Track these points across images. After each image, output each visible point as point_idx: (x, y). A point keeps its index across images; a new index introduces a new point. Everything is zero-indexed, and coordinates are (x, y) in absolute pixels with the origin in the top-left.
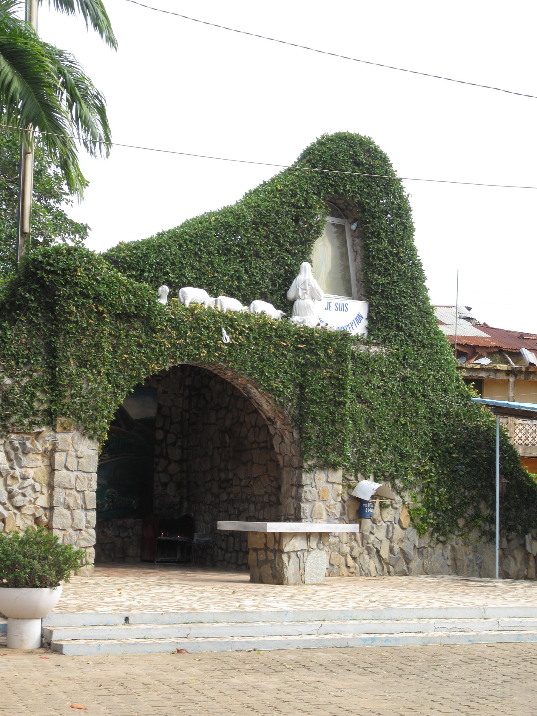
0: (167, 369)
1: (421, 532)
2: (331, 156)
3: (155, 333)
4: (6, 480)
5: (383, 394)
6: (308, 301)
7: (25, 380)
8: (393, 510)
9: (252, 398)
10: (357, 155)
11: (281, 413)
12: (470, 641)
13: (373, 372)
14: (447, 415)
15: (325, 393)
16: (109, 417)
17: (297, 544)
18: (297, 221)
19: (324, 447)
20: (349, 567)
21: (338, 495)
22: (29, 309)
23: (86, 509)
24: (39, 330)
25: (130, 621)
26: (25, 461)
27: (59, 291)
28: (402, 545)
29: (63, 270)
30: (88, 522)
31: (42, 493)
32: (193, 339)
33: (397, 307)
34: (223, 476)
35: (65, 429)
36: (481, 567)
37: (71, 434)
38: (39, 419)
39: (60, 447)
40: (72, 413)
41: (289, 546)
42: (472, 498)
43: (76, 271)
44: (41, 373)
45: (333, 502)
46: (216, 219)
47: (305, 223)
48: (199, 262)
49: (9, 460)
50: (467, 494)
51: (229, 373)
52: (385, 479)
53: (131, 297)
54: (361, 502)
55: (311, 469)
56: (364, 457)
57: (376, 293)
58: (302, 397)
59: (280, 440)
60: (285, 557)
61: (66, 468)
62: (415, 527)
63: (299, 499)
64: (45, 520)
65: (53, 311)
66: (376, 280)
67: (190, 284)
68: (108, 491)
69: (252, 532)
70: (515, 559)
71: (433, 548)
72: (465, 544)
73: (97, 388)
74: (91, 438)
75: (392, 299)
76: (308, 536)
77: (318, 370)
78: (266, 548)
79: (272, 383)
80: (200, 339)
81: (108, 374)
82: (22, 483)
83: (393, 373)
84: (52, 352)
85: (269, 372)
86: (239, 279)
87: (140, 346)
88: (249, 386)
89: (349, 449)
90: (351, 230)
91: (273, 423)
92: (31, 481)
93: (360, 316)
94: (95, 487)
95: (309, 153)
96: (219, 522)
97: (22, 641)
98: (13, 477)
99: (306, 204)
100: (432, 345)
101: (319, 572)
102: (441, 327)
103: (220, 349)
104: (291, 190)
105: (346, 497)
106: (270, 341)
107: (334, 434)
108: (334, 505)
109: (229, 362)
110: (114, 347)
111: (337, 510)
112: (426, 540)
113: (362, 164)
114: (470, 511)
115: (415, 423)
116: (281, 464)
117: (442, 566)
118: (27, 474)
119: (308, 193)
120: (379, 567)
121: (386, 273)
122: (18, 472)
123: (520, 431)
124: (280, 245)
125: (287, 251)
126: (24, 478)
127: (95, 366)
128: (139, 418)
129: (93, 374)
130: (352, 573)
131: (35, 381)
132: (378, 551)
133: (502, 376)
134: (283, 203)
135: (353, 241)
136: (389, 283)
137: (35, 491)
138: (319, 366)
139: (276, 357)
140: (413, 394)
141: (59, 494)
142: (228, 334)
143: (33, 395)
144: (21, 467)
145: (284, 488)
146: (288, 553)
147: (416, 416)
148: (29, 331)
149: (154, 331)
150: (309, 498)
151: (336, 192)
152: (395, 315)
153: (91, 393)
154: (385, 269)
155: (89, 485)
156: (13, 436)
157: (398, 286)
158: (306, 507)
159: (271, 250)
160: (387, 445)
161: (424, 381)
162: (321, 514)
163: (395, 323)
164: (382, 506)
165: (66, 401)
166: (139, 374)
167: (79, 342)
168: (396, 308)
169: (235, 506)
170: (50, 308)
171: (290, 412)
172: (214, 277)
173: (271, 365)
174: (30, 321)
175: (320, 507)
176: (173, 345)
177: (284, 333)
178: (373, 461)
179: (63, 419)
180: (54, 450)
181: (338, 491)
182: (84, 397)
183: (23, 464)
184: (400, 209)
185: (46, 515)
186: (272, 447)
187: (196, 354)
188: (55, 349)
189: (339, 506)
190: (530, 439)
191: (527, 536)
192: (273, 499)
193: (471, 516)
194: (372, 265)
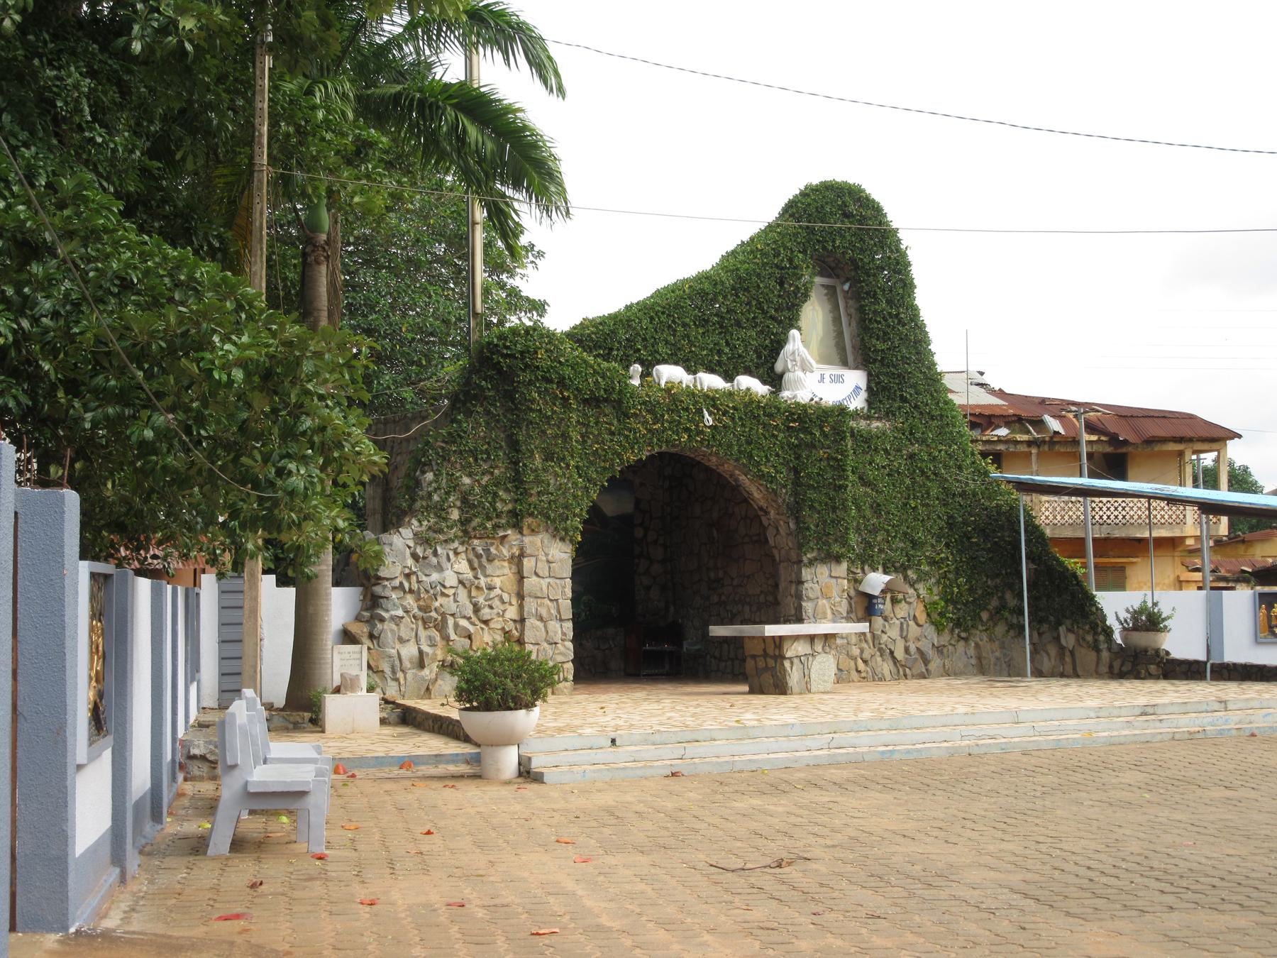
0: (644, 458)
1: (939, 629)
2: (817, 208)
3: (629, 418)
4: (470, 592)
5: (889, 475)
6: (800, 374)
7: (486, 478)
8: (907, 606)
9: (740, 486)
10: (846, 206)
11: (775, 501)
13: (876, 450)
14: (963, 494)
15: (822, 476)
16: (581, 515)
18: (781, 284)
19: (825, 538)
21: (844, 591)
22: (486, 398)
23: (561, 620)
24: (498, 421)
25: (618, 743)
26: (490, 569)
27: (519, 376)
28: (919, 644)
29: (522, 353)
30: (564, 634)
31: (511, 604)
32: (670, 423)
33: (899, 376)
34: (712, 575)
35: (533, 530)
37: (540, 536)
38: (503, 521)
39: (528, 552)
40: (540, 513)
41: (792, 650)
42: (996, 587)
43: (536, 353)
44: (502, 470)
45: (838, 599)
46: (690, 287)
47: (791, 285)
48: (674, 335)
49: (473, 569)
50: (989, 583)
51: (714, 459)
52: (896, 571)
53: (600, 380)
54: (869, 598)
55: (811, 563)
56: (871, 547)
57: (875, 360)
58: (797, 483)
59: (775, 531)
60: (787, 664)
61: (537, 574)
62: (933, 623)
63: (799, 597)
64: (516, 634)
65: (513, 400)
66: (874, 346)
67: (665, 362)
68: (584, 598)
69: (749, 637)
70: (1048, 654)
72: (991, 640)
73: (566, 484)
74: (562, 539)
75: (894, 366)
76: (812, 638)
77: (814, 451)
78: (765, 655)
79: (763, 468)
80: (679, 422)
81: (577, 467)
82: (489, 594)
83: (899, 450)
84: (514, 445)
85: (758, 456)
86: (720, 352)
87: (612, 433)
88: (737, 472)
89: (853, 538)
90: (843, 291)
91: (767, 513)
92: (498, 591)
93: (857, 388)
94: (570, 595)
95: (792, 207)
97: (498, 770)
98: (478, 588)
99: (791, 264)
100: (941, 416)
101: (826, 678)
102: (950, 396)
103: (702, 432)
104: (773, 249)
105: (852, 593)
106: (758, 421)
107: (836, 522)
108: (840, 602)
109: (713, 446)
110: (582, 436)
111: (843, 608)
112: (946, 637)
113: (853, 216)
114: (995, 603)
115: (927, 505)
116: (777, 558)
117: (965, 666)
118: (493, 584)
119: (792, 252)
120: (894, 670)
121: (885, 337)
122: (483, 581)
123: (1047, 509)
124: (764, 312)
125: (772, 318)
126: (491, 588)
127: (563, 459)
128: (615, 515)
129: (561, 468)
131: (496, 478)
132: (892, 653)
133: (1023, 448)
134: (764, 264)
135: (847, 303)
136: (889, 349)
137: (503, 602)
138: (814, 447)
139: (766, 438)
140: (923, 472)
141: (530, 604)
142: (710, 415)
143: (495, 495)
144: (486, 576)
145: (782, 586)
147: (928, 498)
148: (487, 424)
149: (627, 416)
150: (811, 595)
151: (824, 248)
152: (898, 384)
153: (560, 489)
154: (884, 332)
155: (563, 593)
156: (476, 542)
157: (899, 351)
158: (808, 606)
159: (754, 318)
160: (896, 531)
161: (935, 458)
162: (825, 613)
163: (898, 393)
164: (894, 601)
165: (533, 499)
166: (613, 465)
167: (544, 432)
168: (899, 376)
169: (728, 608)
170: (509, 396)
171: (784, 500)
172: (691, 351)
173: (761, 448)
174: (488, 412)
175: (824, 605)
176: (650, 431)
177: (774, 411)
178: (881, 551)
179: (530, 520)
180: (522, 555)
182: (552, 494)
183: (488, 573)
184: (898, 263)
185: (516, 629)
186: (767, 541)
187: (675, 440)
188: (517, 442)
189: (845, 603)
190: (1059, 517)
192: (770, 598)
193: (996, 608)
194: (869, 329)
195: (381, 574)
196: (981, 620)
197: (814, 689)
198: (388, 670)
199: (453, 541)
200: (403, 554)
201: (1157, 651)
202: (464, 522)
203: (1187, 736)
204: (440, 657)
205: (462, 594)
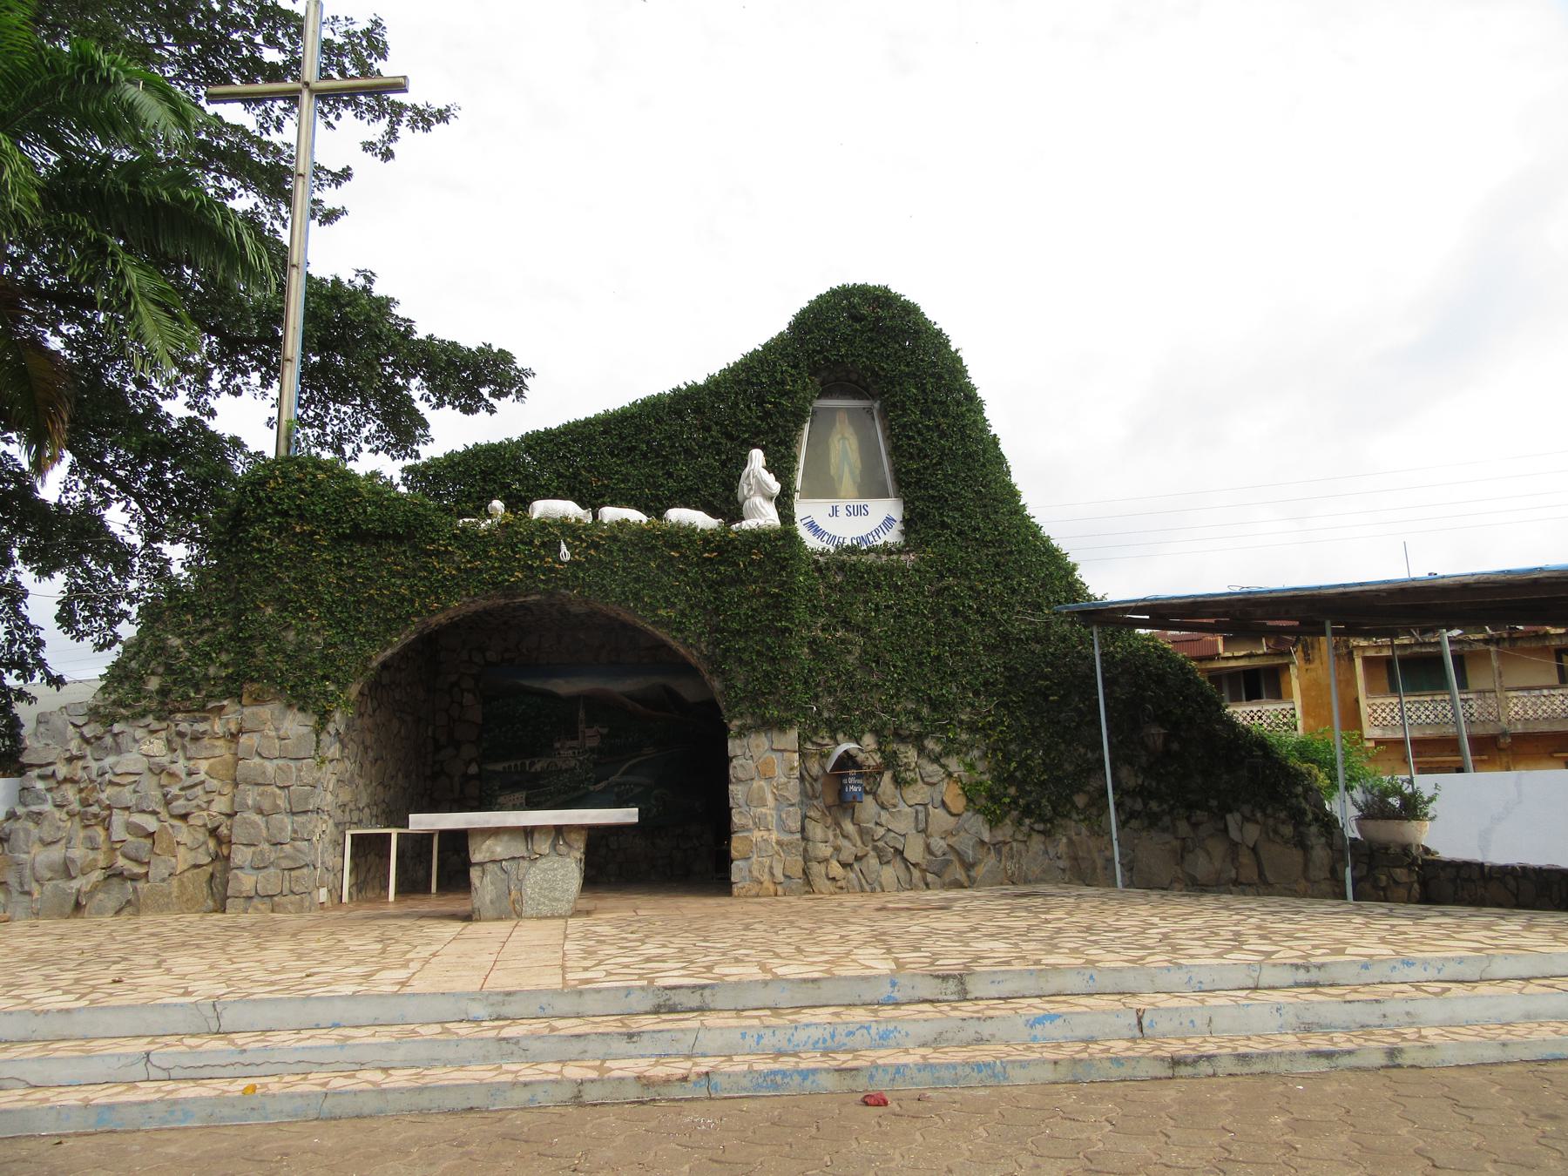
1: (994, 822)
8: (926, 788)
17: (499, 848)
20: (834, 879)
36: (1132, 869)
45: (784, 780)
50: (1089, 755)
55: (741, 734)
68: (655, 792)
70: (1208, 853)
74: (302, 709)
75: (933, 487)
93: (889, 521)
101: (557, 894)
123: (1516, 705)
130: (841, 888)
132: (899, 853)
133: (1480, 647)
140: (955, 612)
146: (481, 864)
150: (740, 775)
175: (761, 788)
181: (791, 761)
189: (794, 785)
190: (1531, 712)
191: (1229, 817)
195: (24, 759)
196: (1074, 806)
197: (527, 910)
198: (12, 880)
199: (143, 716)
200: (63, 734)
201: (1406, 848)
202: (163, 692)
203: (633, 1092)
204: (102, 864)
205: (150, 785)
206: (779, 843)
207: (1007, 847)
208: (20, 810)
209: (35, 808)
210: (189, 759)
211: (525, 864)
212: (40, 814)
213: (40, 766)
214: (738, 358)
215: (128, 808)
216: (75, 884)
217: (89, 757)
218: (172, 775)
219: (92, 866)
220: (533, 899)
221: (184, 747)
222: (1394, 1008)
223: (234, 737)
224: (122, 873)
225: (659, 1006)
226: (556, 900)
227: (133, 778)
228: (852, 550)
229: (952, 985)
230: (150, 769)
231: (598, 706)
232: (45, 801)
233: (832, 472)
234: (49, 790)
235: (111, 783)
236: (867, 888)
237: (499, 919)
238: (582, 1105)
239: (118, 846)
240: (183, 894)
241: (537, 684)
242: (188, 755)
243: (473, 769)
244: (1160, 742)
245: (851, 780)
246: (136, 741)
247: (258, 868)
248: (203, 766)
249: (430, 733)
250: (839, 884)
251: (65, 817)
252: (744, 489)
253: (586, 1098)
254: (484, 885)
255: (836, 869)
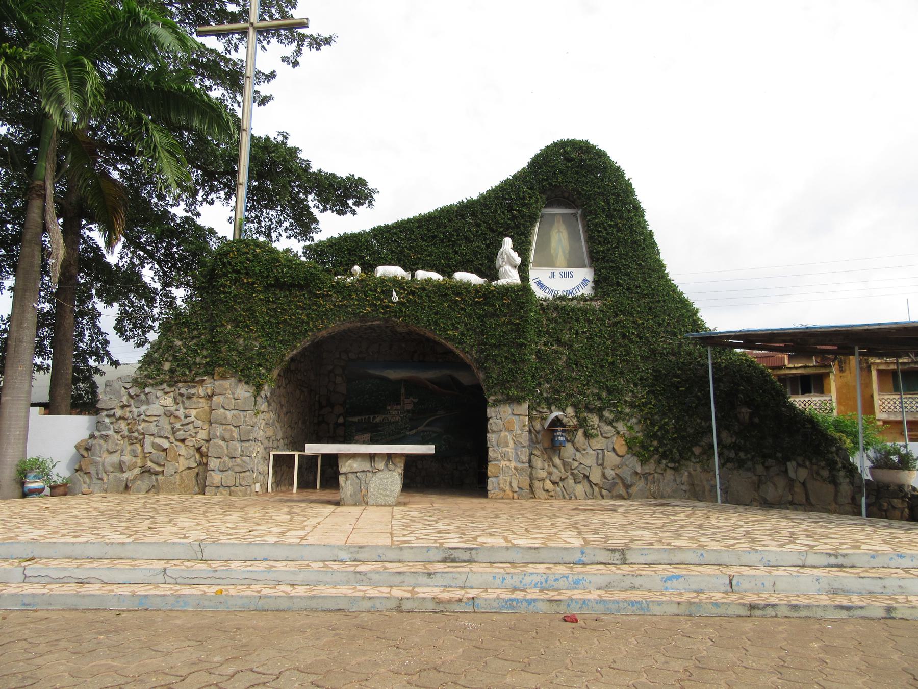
1: (644, 461)
8: (604, 440)
12: (24, 605)
17: (355, 465)
20: (547, 491)
36: (727, 492)
45: (519, 432)
55: (495, 404)
70: (775, 485)
71: (662, 474)
74: (247, 383)
75: (612, 262)
93: (585, 281)
96: (433, 452)
101: (388, 493)
130: (552, 496)
132: (586, 477)
140: (624, 336)
146: (345, 474)
150: (494, 428)
175: (506, 437)
189: (526, 435)
191: (789, 464)
195: (99, 406)
196: (693, 453)
197: (371, 501)
198: (93, 472)
199: (161, 384)
200: (119, 392)
201: (901, 487)
202: (172, 371)
203: (431, 606)
204: (139, 465)
205: (164, 423)
206: (515, 468)
207: (652, 476)
208: (97, 434)
209: (104, 433)
210: (186, 409)
211: (369, 474)
212: (107, 436)
213: (107, 410)
214: (497, 183)
215: (153, 435)
216: (125, 475)
217: (133, 406)
218: (176, 417)
219: (134, 466)
220: (374, 495)
221: (183, 402)
222: (892, 583)
223: (210, 397)
224: (150, 470)
225: (446, 558)
226: (387, 496)
227: (155, 418)
228: (563, 298)
229: (617, 555)
230: (165, 414)
231: (412, 386)
232: (109, 429)
233: (552, 251)
234: (112, 423)
235: (144, 420)
236: (567, 497)
237: (355, 505)
238: (401, 611)
239: (148, 455)
240: (182, 483)
241: (378, 373)
242: (185, 406)
243: (341, 420)
244: (747, 417)
245: (559, 434)
246: (157, 398)
247: (222, 471)
248: (193, 413)
249: (317, 399)
250: (550, 494)
251: (120, 438)
252: (499, 261)
253: (404, 608)
254: (347, 486)
255: (549, 485)
